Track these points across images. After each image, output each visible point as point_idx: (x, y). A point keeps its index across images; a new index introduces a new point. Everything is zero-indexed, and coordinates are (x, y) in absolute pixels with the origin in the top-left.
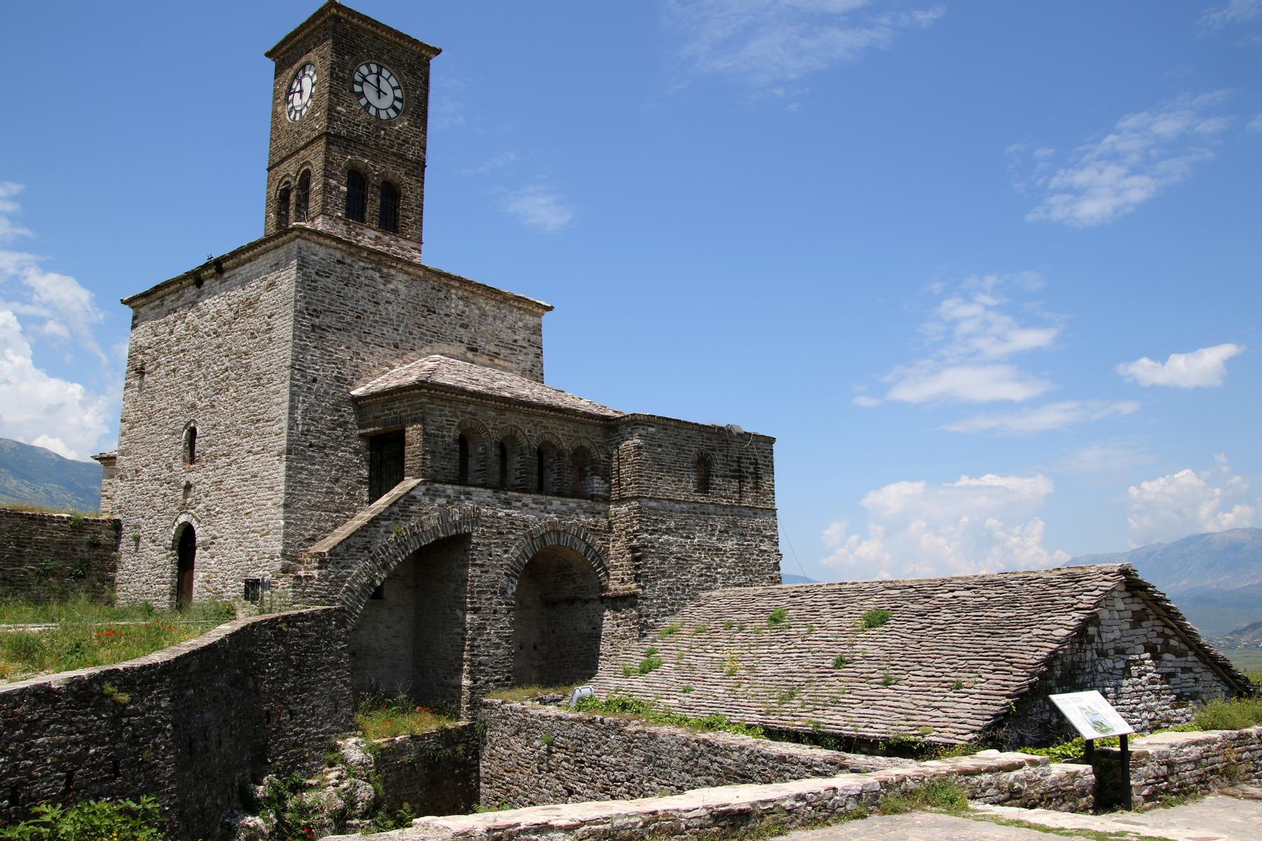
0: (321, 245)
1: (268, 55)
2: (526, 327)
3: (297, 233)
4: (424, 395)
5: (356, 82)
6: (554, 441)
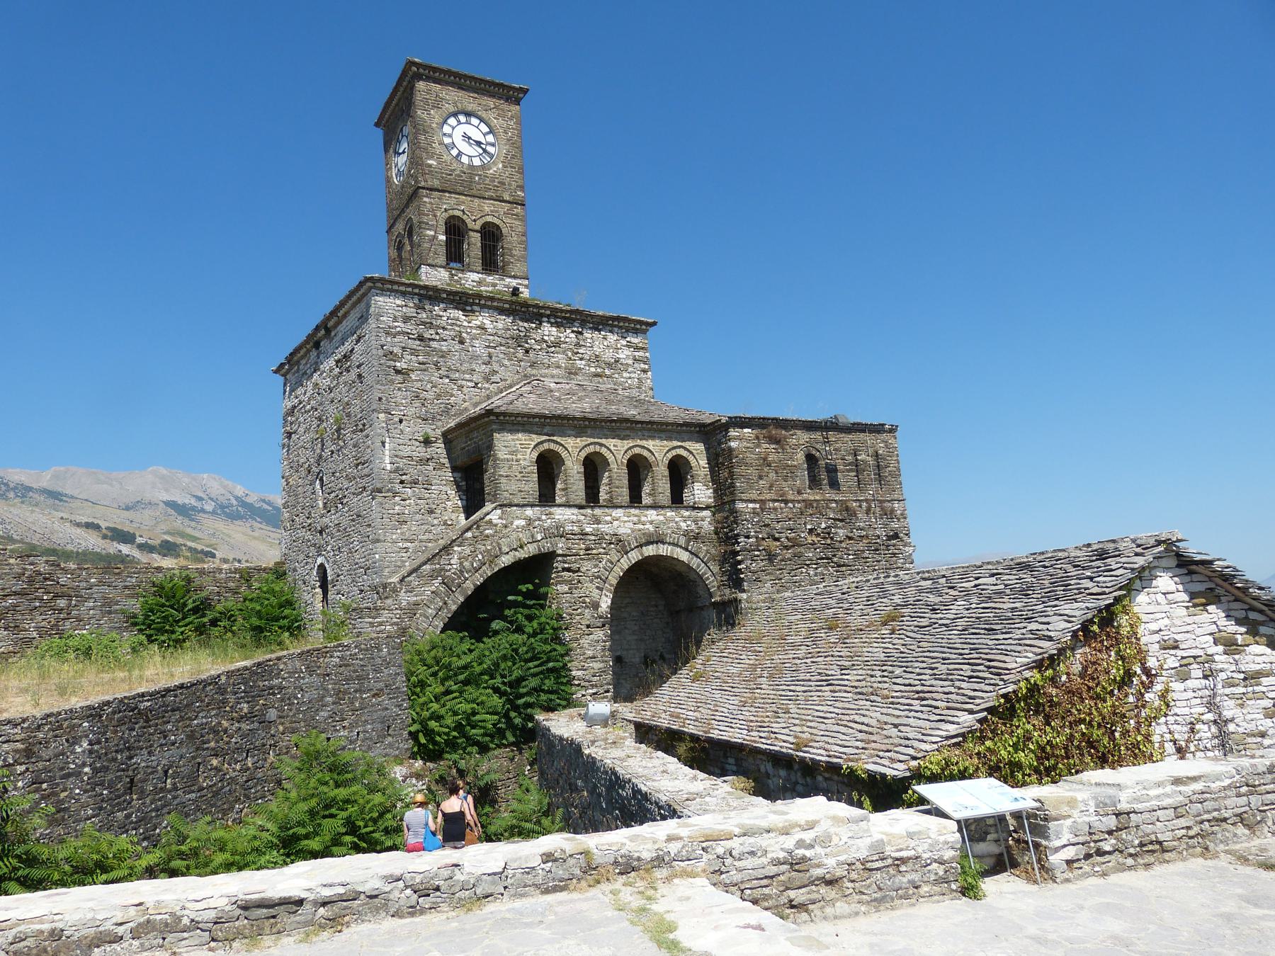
1: (377, 125)
4: (492, 422)
6: (645, 453)
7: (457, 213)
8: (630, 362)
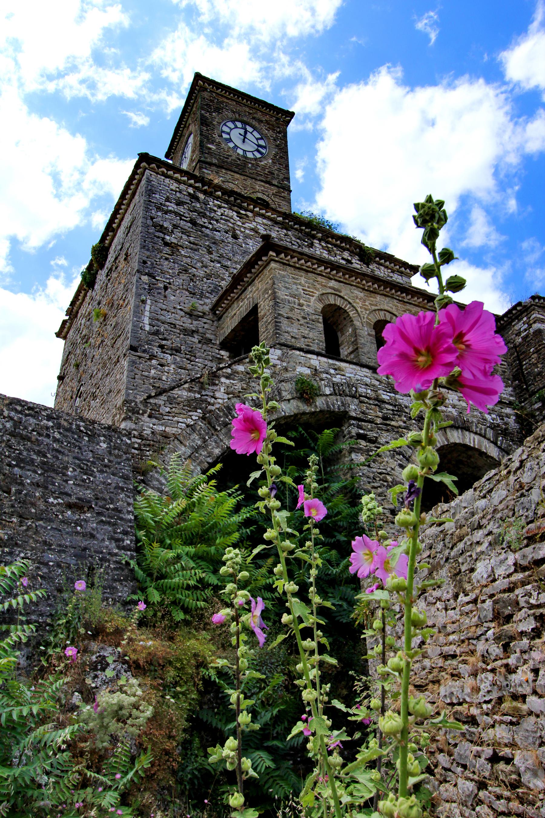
3: (144, 164)
5: (223, 132)
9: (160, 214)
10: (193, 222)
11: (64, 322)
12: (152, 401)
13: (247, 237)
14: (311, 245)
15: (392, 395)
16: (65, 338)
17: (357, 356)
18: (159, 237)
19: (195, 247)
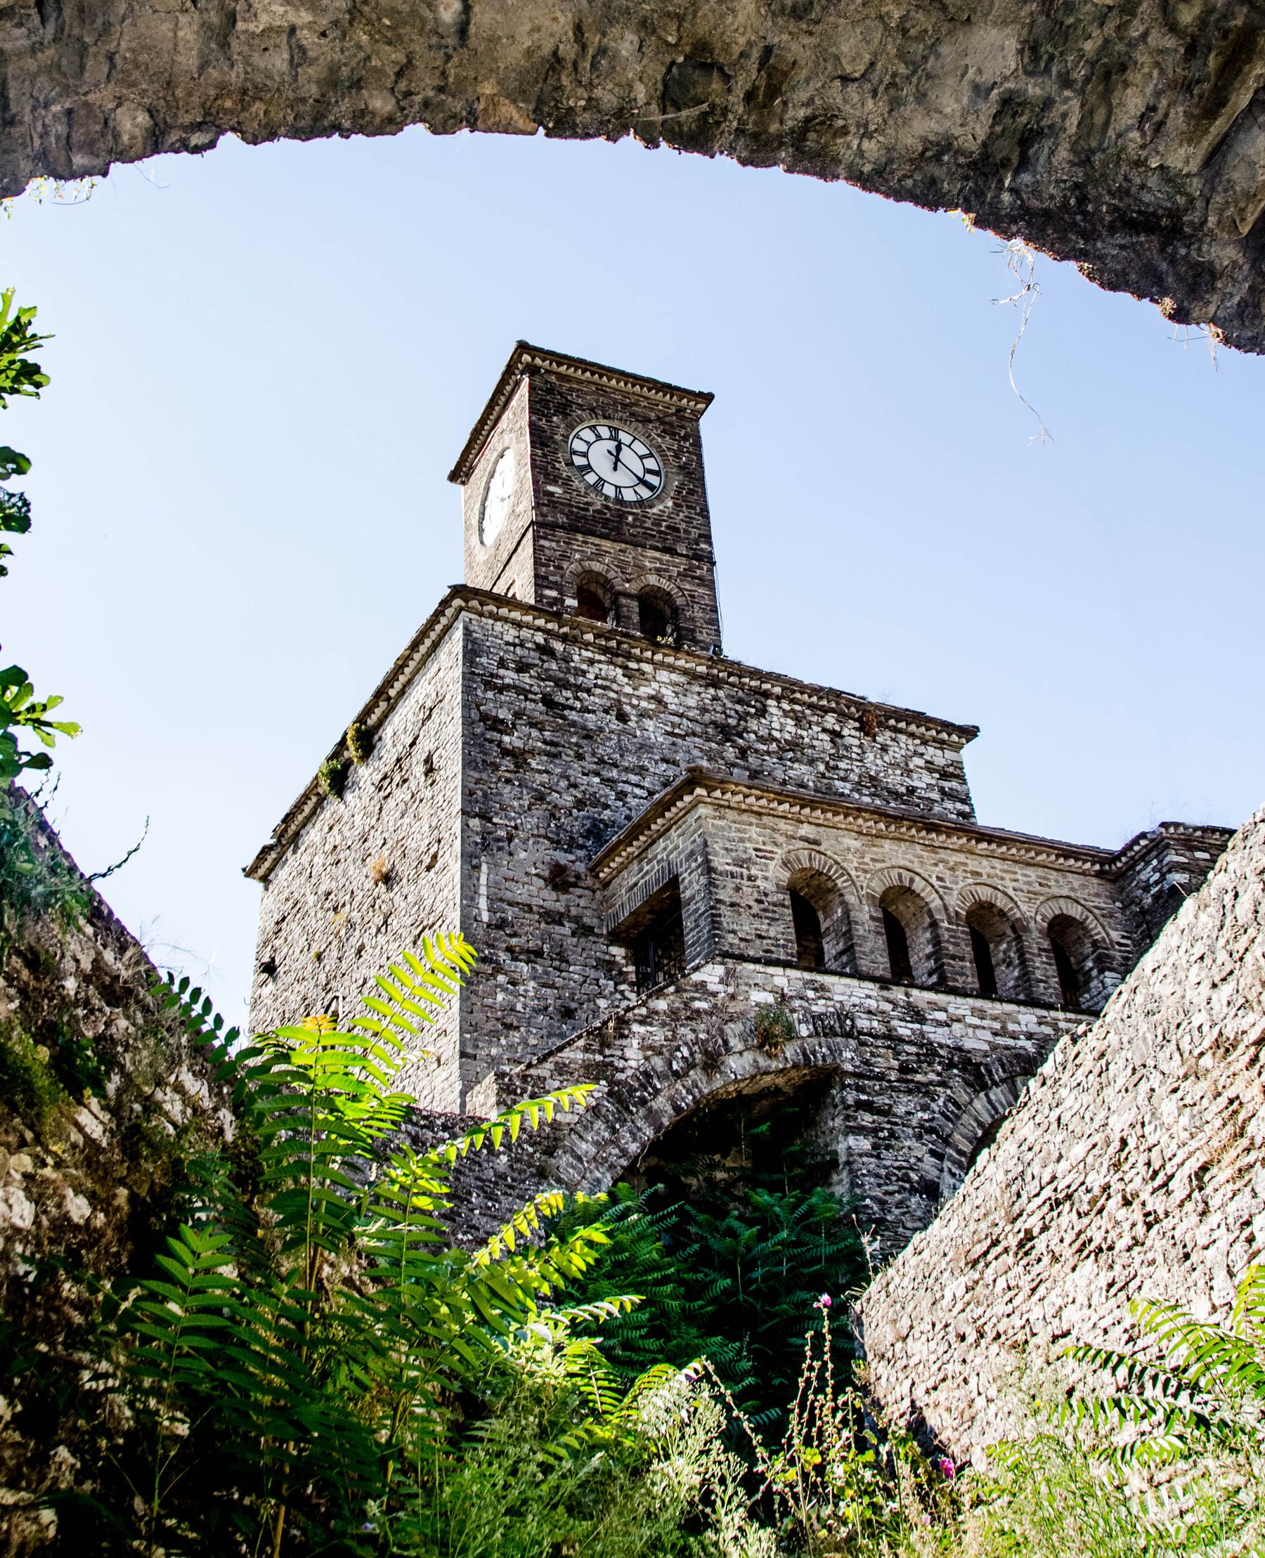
0: (506, 620)
2: (930, 767)
3: (457, 602)
5: (575, 453)
6: (1001, 902)
7: (596, 566)
8: (935, 795)
9: (490, 694)
10: (548, 701)
11: (266, 850)
12: (532, 1071)
13: (643, 715)
14: (762, 712)
15: (917, 1026)
16: (265, 879)
17: (853, 960)
18: (491, 741)
19: (553, 750)
